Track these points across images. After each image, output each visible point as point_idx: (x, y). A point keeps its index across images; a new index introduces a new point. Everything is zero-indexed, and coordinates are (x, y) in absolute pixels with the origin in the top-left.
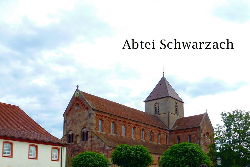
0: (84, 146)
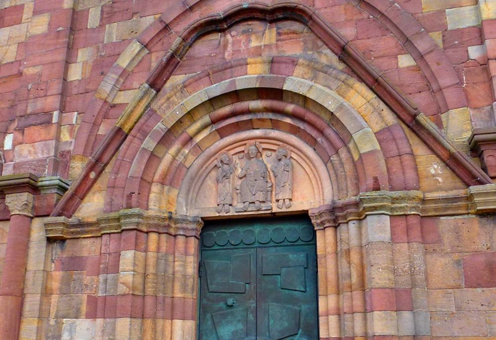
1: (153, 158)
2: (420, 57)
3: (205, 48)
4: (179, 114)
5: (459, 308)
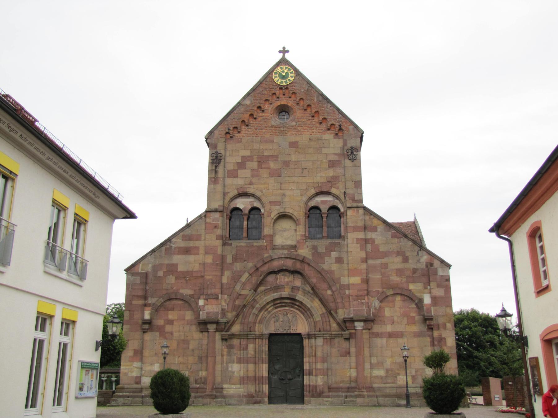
0: (326, 259)
1: (257, 316)
2: (333, 292)
3: (271, 278)
4: (265, 303)
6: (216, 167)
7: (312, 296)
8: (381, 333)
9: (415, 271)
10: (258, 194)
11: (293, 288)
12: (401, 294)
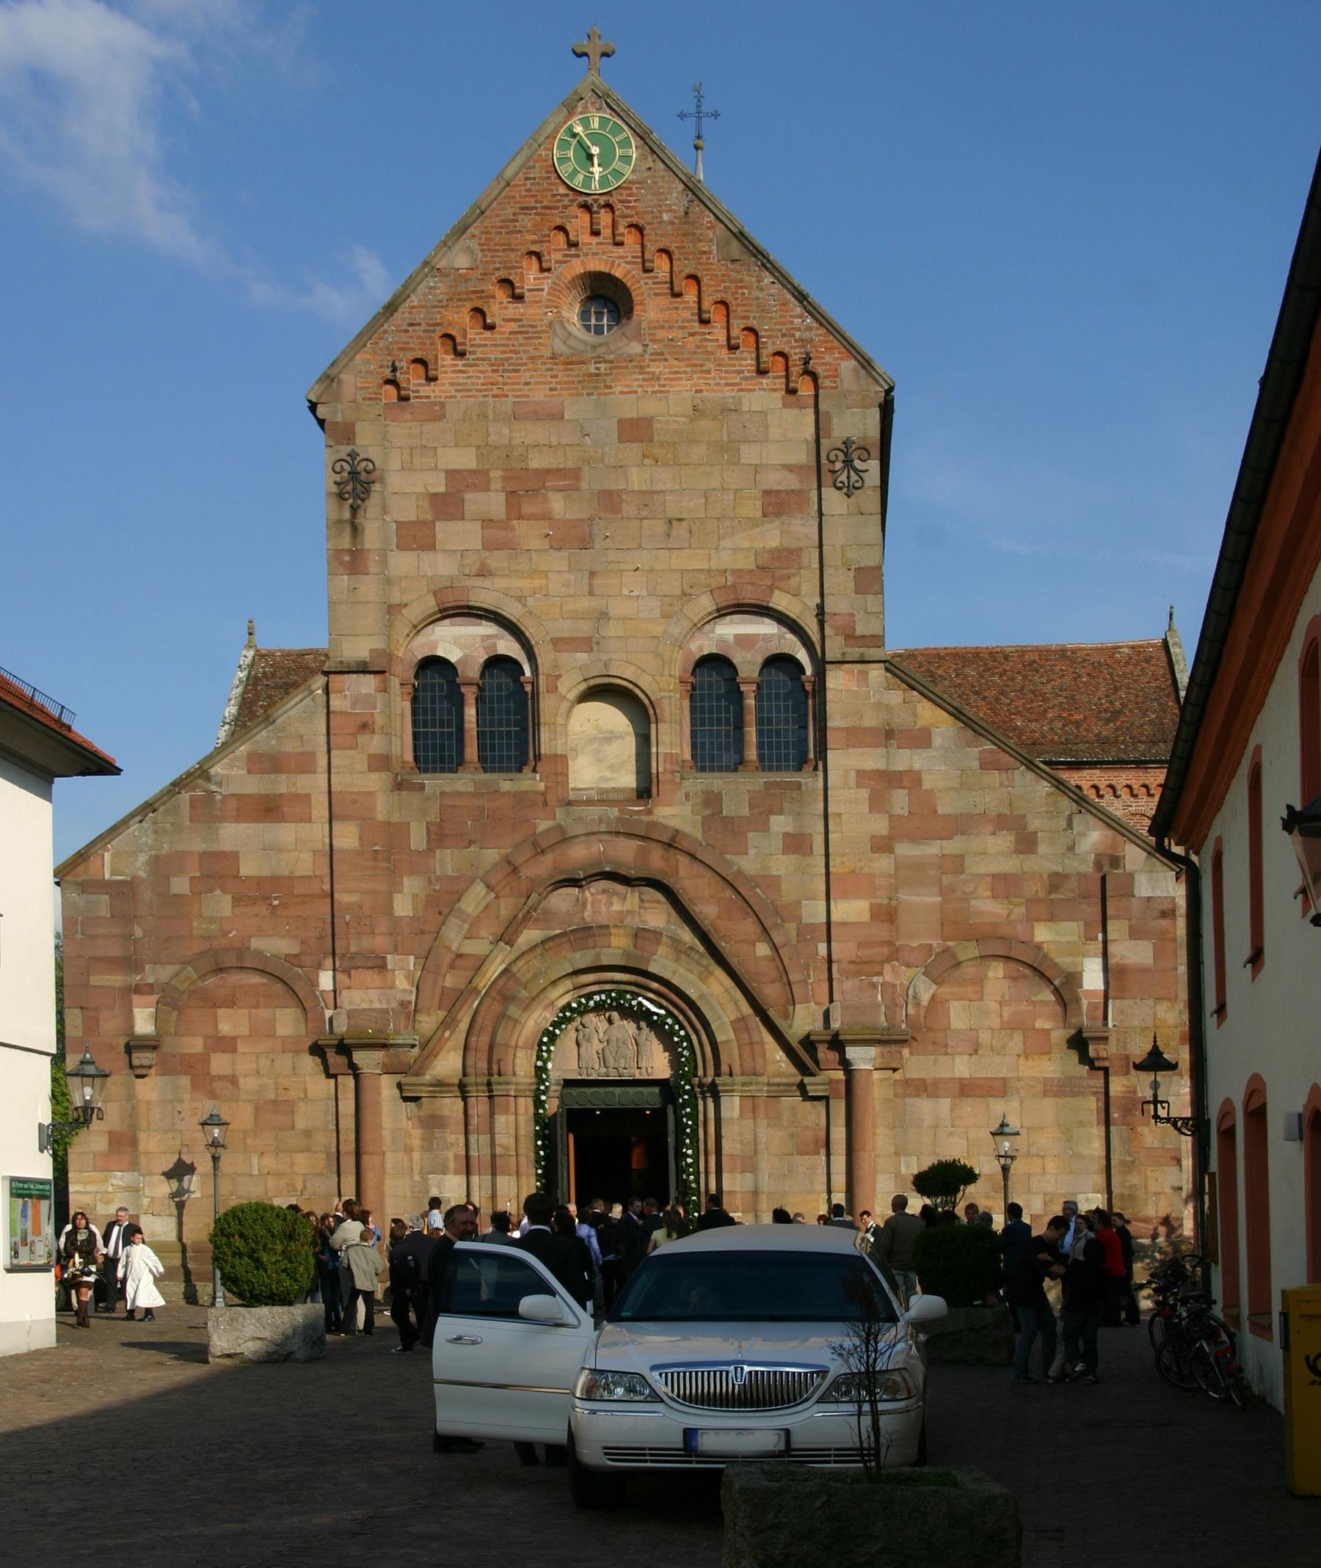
2: (775, 948)
5: (790, 1171)
6: (354, 509)
7: (705, 962)
8: (936, 1082)
9: (1056, 881)
10: (511, 610)
11: (640, 935)
12: (1008, 958)
